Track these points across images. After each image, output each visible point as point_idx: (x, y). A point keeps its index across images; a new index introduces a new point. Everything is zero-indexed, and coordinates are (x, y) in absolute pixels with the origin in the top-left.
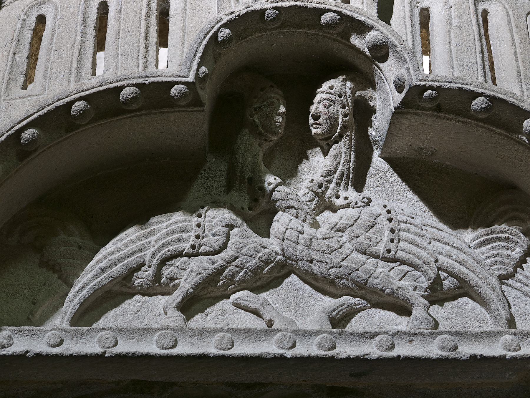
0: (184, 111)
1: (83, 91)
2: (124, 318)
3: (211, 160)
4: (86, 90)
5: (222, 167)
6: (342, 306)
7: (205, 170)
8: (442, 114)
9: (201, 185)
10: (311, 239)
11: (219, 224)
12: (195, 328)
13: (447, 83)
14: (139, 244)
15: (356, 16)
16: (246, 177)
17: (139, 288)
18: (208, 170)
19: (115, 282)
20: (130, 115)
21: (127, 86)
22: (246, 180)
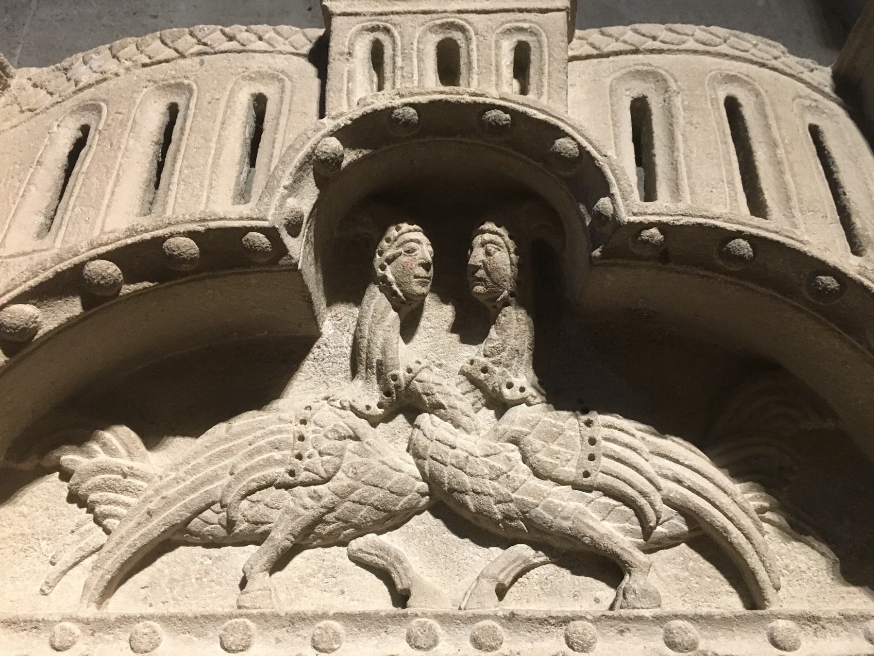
0: (267, 271)
1: (100, 245)
2: (183, 587)
4: (107, 244)
5: (345, 344)
6: (514, 561)
7: (319, 347)
8: (671, 265)
9: (313, 369)
10: (467, 457)
11: (330, 436)
12: (282, 614)
13: (681, 217)
14: (209, 470)
15: (531, 112)
16: (375, 361)
17: (211, 538)
18: (323, 347)
19: (174, 530)
20: (184, 280)
21: (169, 237)
22: (375, 365)
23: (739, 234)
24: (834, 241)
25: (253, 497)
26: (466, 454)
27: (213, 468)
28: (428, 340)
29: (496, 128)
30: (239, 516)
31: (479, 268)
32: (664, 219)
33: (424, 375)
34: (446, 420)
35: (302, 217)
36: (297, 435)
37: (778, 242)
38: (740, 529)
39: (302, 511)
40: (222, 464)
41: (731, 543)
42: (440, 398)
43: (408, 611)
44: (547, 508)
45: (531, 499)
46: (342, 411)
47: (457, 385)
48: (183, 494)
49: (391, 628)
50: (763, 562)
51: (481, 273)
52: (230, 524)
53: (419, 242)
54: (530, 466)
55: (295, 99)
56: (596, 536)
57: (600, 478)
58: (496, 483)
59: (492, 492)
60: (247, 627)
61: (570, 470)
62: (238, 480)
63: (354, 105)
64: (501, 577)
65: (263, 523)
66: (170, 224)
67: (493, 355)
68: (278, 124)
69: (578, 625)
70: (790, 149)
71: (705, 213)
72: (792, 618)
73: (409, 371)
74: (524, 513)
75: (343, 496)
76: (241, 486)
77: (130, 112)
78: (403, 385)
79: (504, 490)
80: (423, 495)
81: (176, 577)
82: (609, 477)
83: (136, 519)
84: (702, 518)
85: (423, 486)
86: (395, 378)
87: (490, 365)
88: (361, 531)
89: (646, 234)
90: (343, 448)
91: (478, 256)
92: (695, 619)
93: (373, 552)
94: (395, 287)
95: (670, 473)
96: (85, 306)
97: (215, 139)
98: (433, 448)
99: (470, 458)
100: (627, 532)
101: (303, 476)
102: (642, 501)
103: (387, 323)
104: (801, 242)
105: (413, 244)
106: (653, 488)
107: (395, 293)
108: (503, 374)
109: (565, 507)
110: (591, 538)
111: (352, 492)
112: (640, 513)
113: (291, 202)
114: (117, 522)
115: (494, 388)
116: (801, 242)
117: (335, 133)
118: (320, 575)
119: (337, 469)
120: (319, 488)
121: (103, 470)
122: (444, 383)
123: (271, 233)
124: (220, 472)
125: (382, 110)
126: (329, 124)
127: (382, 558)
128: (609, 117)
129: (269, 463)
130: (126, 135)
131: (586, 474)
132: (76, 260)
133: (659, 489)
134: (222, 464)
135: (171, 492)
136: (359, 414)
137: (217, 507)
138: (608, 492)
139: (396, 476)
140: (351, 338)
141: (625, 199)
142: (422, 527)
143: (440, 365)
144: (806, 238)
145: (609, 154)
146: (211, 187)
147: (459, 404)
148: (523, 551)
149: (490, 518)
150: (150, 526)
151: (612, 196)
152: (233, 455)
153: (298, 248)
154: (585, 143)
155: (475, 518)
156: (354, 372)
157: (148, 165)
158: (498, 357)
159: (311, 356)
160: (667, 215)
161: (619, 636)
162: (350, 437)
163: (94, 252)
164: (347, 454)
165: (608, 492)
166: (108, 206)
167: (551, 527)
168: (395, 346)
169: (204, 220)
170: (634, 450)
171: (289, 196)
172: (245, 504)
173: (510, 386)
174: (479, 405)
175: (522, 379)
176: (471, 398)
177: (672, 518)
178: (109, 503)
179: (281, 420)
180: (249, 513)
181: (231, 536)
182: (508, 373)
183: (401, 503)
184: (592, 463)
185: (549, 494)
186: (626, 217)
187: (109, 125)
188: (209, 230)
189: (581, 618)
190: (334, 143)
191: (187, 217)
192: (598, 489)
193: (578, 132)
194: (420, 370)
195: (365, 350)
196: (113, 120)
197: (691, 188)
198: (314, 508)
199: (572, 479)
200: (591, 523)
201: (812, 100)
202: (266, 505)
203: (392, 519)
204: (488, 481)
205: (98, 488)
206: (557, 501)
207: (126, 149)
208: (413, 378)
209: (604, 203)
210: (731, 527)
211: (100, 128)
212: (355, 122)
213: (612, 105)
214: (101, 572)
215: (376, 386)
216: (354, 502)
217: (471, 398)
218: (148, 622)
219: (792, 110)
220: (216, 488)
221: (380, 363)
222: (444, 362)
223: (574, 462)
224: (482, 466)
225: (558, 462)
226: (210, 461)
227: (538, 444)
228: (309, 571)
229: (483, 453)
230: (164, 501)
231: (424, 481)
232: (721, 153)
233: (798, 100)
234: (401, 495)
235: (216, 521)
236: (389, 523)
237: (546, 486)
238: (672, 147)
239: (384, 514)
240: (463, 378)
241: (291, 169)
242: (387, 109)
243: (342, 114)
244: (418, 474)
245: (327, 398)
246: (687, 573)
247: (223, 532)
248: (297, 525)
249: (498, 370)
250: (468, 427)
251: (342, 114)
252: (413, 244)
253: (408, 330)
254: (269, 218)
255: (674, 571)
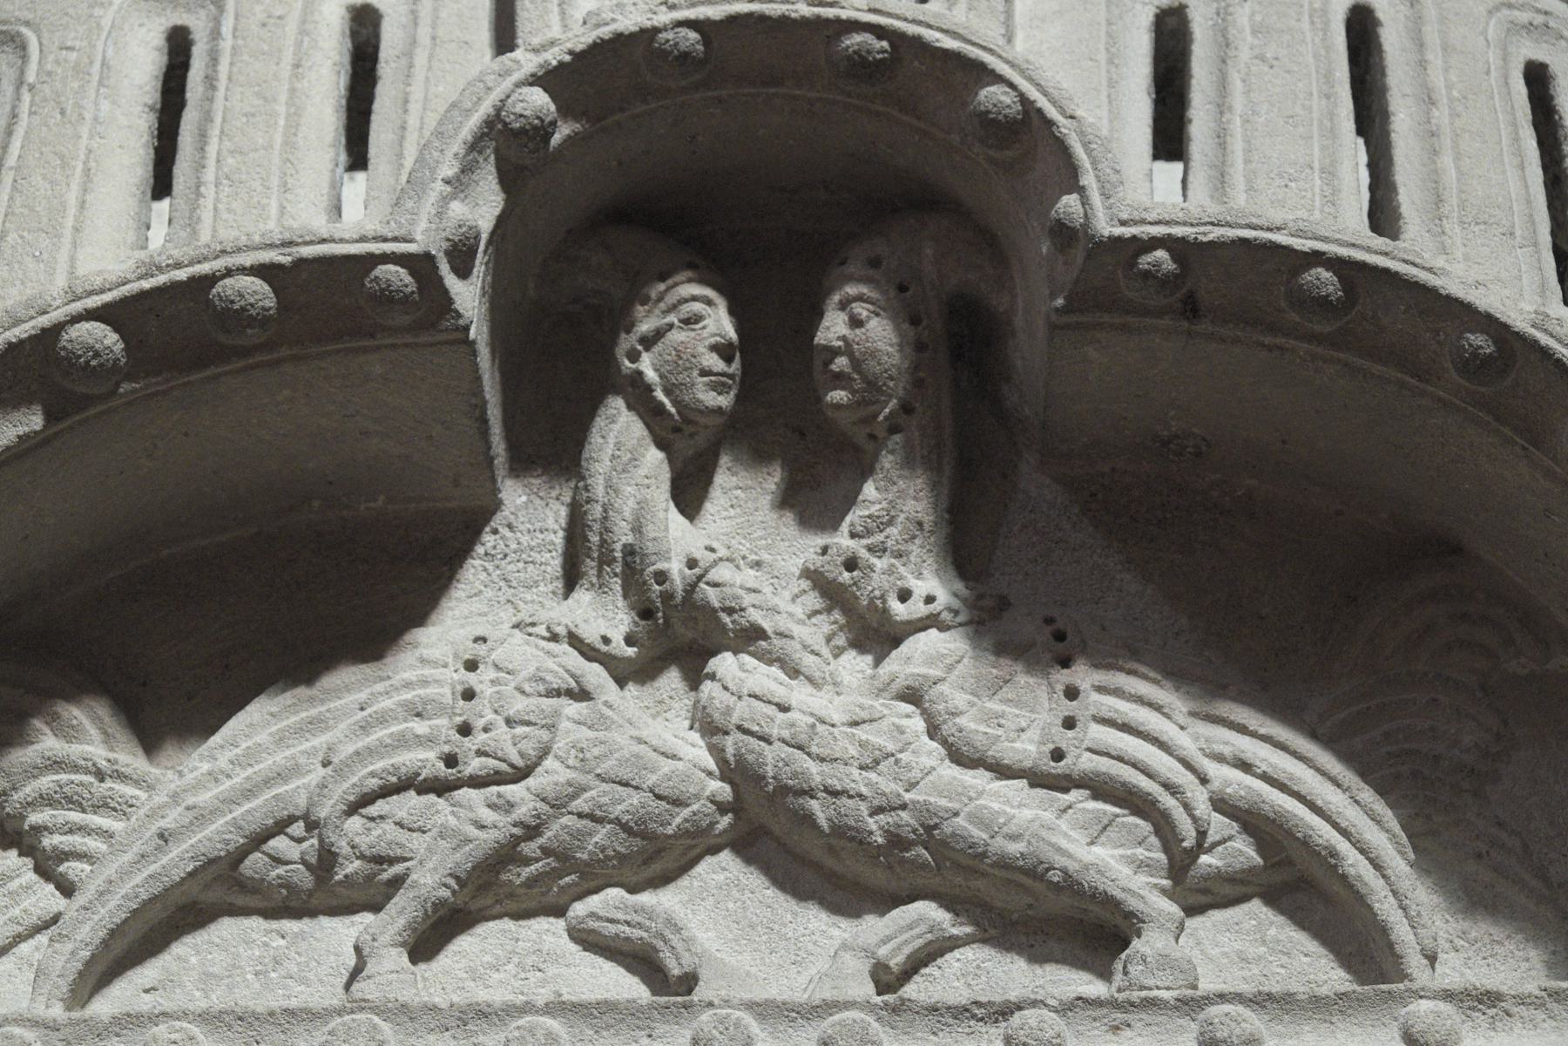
0: (406, 345)
1: (90, 293)
2: (230, 988)
3: (514, 495)
4: (102, 291)
5: (551, 523)
6: (910, 927)
7: (495, 532)
8: (1204, 326)
9: (483, 576)
10: (813, 726)
11: (527, 689)
12: (444, 1006)
13: (1210, 228)
14: (280, 758)
15: (930, 35)
16: (618, 546)
17: (284, 892)
18: (504, 531)
20: (241, 364)
21: (223, 277)
22: (618, 555)
23: (1316, 258)
24: (1520, 278)
25: (372, 810)
26: (811, 720)
27: (287, 753)
28: (732, 512)
29: (861, 65)
30: (343, 847)
31: (833, 353)
32: (1178, 231)
33: (722, 573)
34: (770, 663)
35: (477, 237)
36: (459, 688)
37: (1386, 271)
38: (1362, 851)
39: (473, 832)
40: (306, 746)
41: (1344, 877)
42: (756, 616)
43: (695, 998)
44: (975, 818)
45: (943, 802)
46: (552, 646)
47: (795, 598)
48: (231, 801)
49: (661, 1029)
50: (1404, 909)
51: (841, 363)
52: (327, 860)
53: (709, 302)
54: (944, 742)
55: (443, 14)
56: (1072, 866)
57: (1088, 763)
58: (872, 776)
59: (864, 790)
60: (375, 1027)
61: (1027, 750)
62: (340, 773)
63: (577, 29)
64: (883, 952)
65: (392, 861)
66: (224, 252)
67: (869, 532)
68: (411, 66)
69: (1030, 1016)
70: (1460, 109)
71: (1254, 220)
72: (1448, 995)
73: (692, 563)
74: (929, 829)
75: (558, 804)
76: (346, 785)
77: (92, 46)
78: (680, 594)
79: (888, 786)
80: (722, 808)
81: (215, 970)
82: (1105, 760)
83: (137, 848)
84: (1289, 833)
85: (722, 789)
86: (662, 577)
87: (863, 553)
88: (594, 878)
89: (1145, 261)
90: (557, 713)
91: (833, 328)
92: (1260, 1001)
93: (620, 916)
94: (659, 395)
95: (1227, 751)
96: (50, 417)
97: (283, 98)
98: (742, 711)
99: (820, 728)
100: (1141, 866)
101: (474, 766)
102: (1168, 801)
103: (642, 472)
104: (1430, 270)
105: (697, 307)
106: (1191, 777)
107: (659, 409)
108: (890, 571)
109: (1015, 817)
110: (1064, 871)
111: (574, 796)
112: (1163, 826)
113: (457, 209)
114: (88, 868)
115: (872, 601)
116: (1430, 270)
117: (535, 80)
118: (510, 967)
119: (545, 752)
120: (510, 790)
121: (57, 765)
122: (767, 590)
123: (420, 265)
124: (302, 760)
125: (632, 35)
126: (525, 61)
127: (640, 926)
128: (1102, 47)
129: (404, 741)
130: (92, 93)
131: (1058, 755)
132: (44, 321)
133: (1204, 781)
134: (306, 746)
135: (204, 798)
136: (588, 652)
137: (298, 829)
138: (1101, 788)
139: (667, 766)
140: (564, 512)
141: (1106, 196)
142: (721, 877)
143: (757, 564)
144: (1440, 262)
145: (1079, 113)
146: (285, 188)
147: (797, 630)
148: (928, 911)
149: (861, 842)
150: (165, 860)
151: (1082, 191)
152: (327, 729)
153: (468, 296)
154: (1033, 94)
155: (831, 849)
156: (571, 579)
157: (142, 152)
158: (880, 537)
159: (480, 550)
160: (1185, 224)
161: (1110, 1036)
162: (569, 693)
163: (78, 306)
164: (565, 725)
165: (1101, 788)
166: (76, 230)
167: (984, 855)
168: (661, 515)
169: (291, 243)
170: (1157, 708)
171: (453, 197)
172: (355, 823)
173: (904, 596)
174: (841, 640)
175: (929, 585)
176: (824, 624)
177: (1230, 838)
178: (71, 831)
179: (423, 661)
180: (364, 842)
181: (326, 891)
182: (902, 569)
183: (678, 820)
184: (1070, 734)
185: (980, 794)
186: (1105, 227)
187: (49, 74)
188: (301, 262)
189: (1034, 1003)
190: (539, 100)
191: (257, 238)
192: (1079, 784)
193: (1022, 72)
194: (715, 563)
195: (596, 527)
196: (57, 62)
197: (1248, 181)
198: (500, 827)
199: (1028, 764)
200: (1064, 843)
201: (1538, 11)
202: (400, 824)
203: (657, 856)
204: (856, 772)
205: (46, 800)
206: (996, 806)
207: (96, 119)
208: (700, 578)
209: (1069, 204)
210: (1343, 846)
211: (31, 77)
212: (578, 56)
213: (1109, 23)
214: (69, 946)
215: (621, 603)
216: (580, 815)
217: (824, 624)
218: (178, 1024)
219: (1484, 33)
220: (297, 792)
221: (629, 551)
222: (765, 556)
223: (1034, 733)
224: (843, 743)
225: (1000, 732)
226: (280, 740)
227: (960, 699)
228: (487, 958)
229: (846, 718)
230: (191, 814)
231: (722, 779)
232: (1315, 115)
233: (1505, 12)
234: (678, 803)
235: (296, 856)
236: (656, 868)
237: (977, 779)
238: (1222, 106)
239: (638, 842)
240: (805, 584)
241: (457, 146)
242: (643, 31)
243: (553, 43)
244: (711, 764)
245: (516, 626)
246: (1263, 949)
247: (304, 878)
248: (463, 859)
249: (879, 564)
250: (817, 674)
251: (553, 43)
252: (697, 307)
253: (689, 493)
254: (419, 237)
255: (1237, 946)
